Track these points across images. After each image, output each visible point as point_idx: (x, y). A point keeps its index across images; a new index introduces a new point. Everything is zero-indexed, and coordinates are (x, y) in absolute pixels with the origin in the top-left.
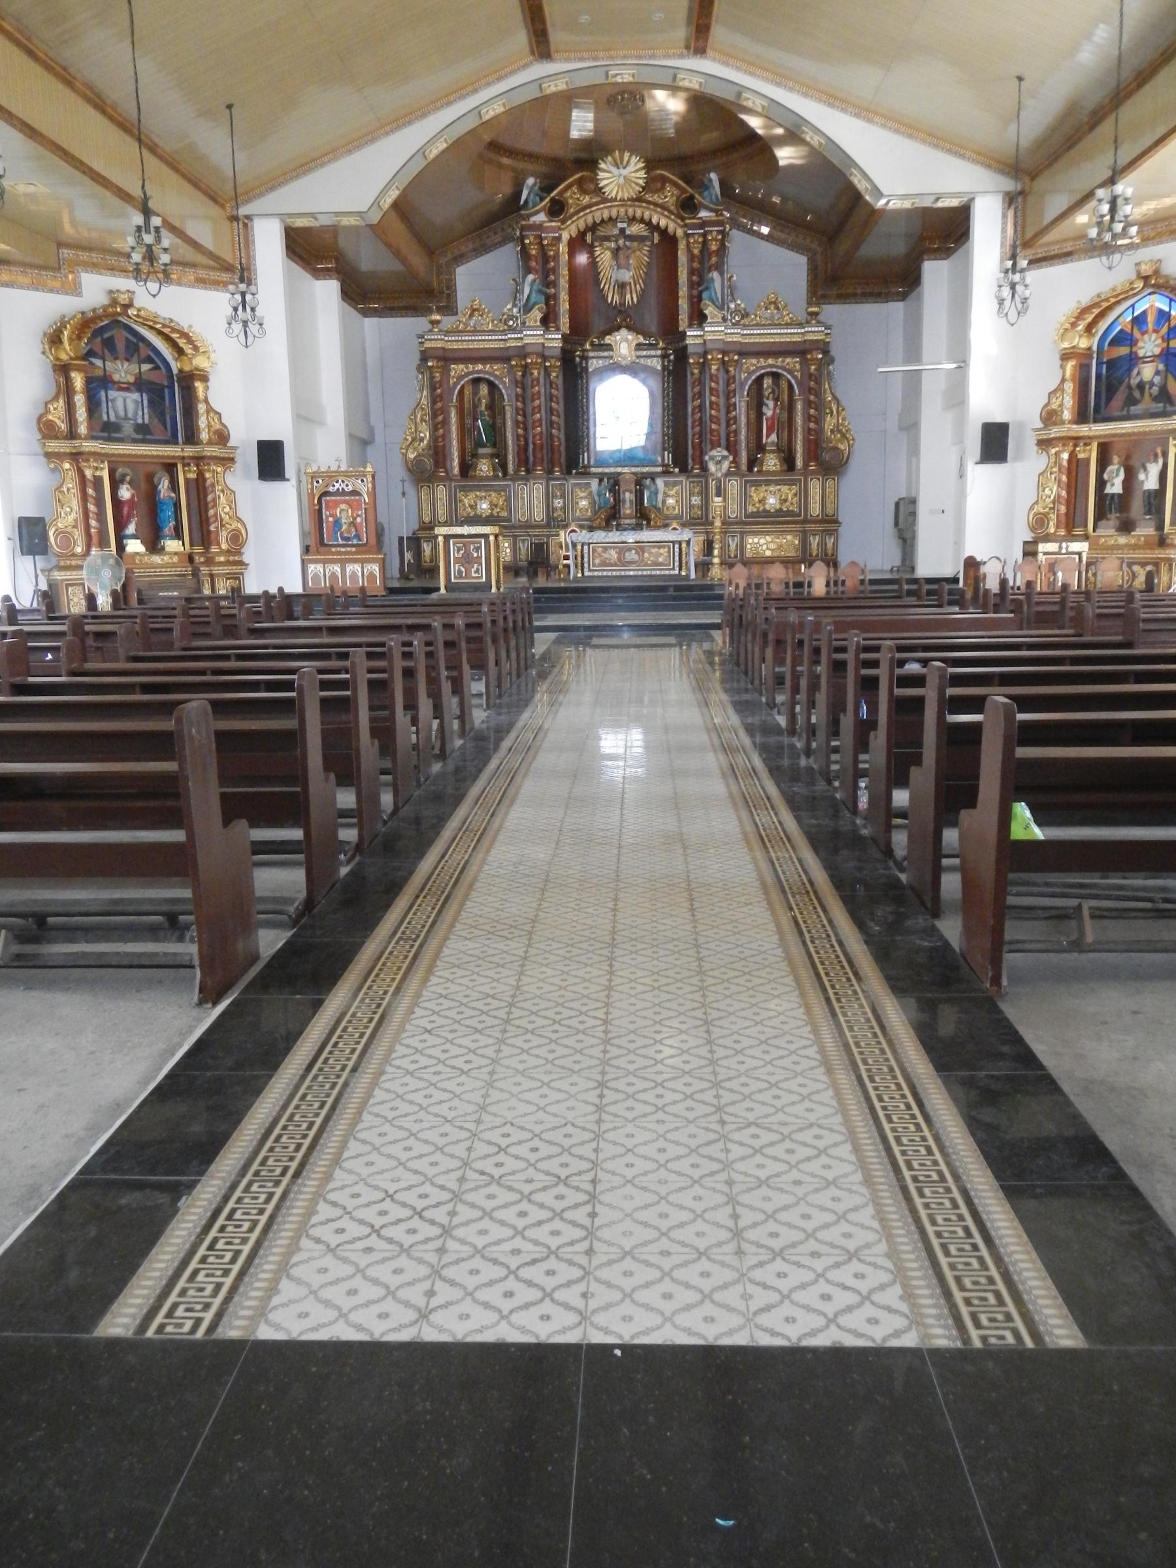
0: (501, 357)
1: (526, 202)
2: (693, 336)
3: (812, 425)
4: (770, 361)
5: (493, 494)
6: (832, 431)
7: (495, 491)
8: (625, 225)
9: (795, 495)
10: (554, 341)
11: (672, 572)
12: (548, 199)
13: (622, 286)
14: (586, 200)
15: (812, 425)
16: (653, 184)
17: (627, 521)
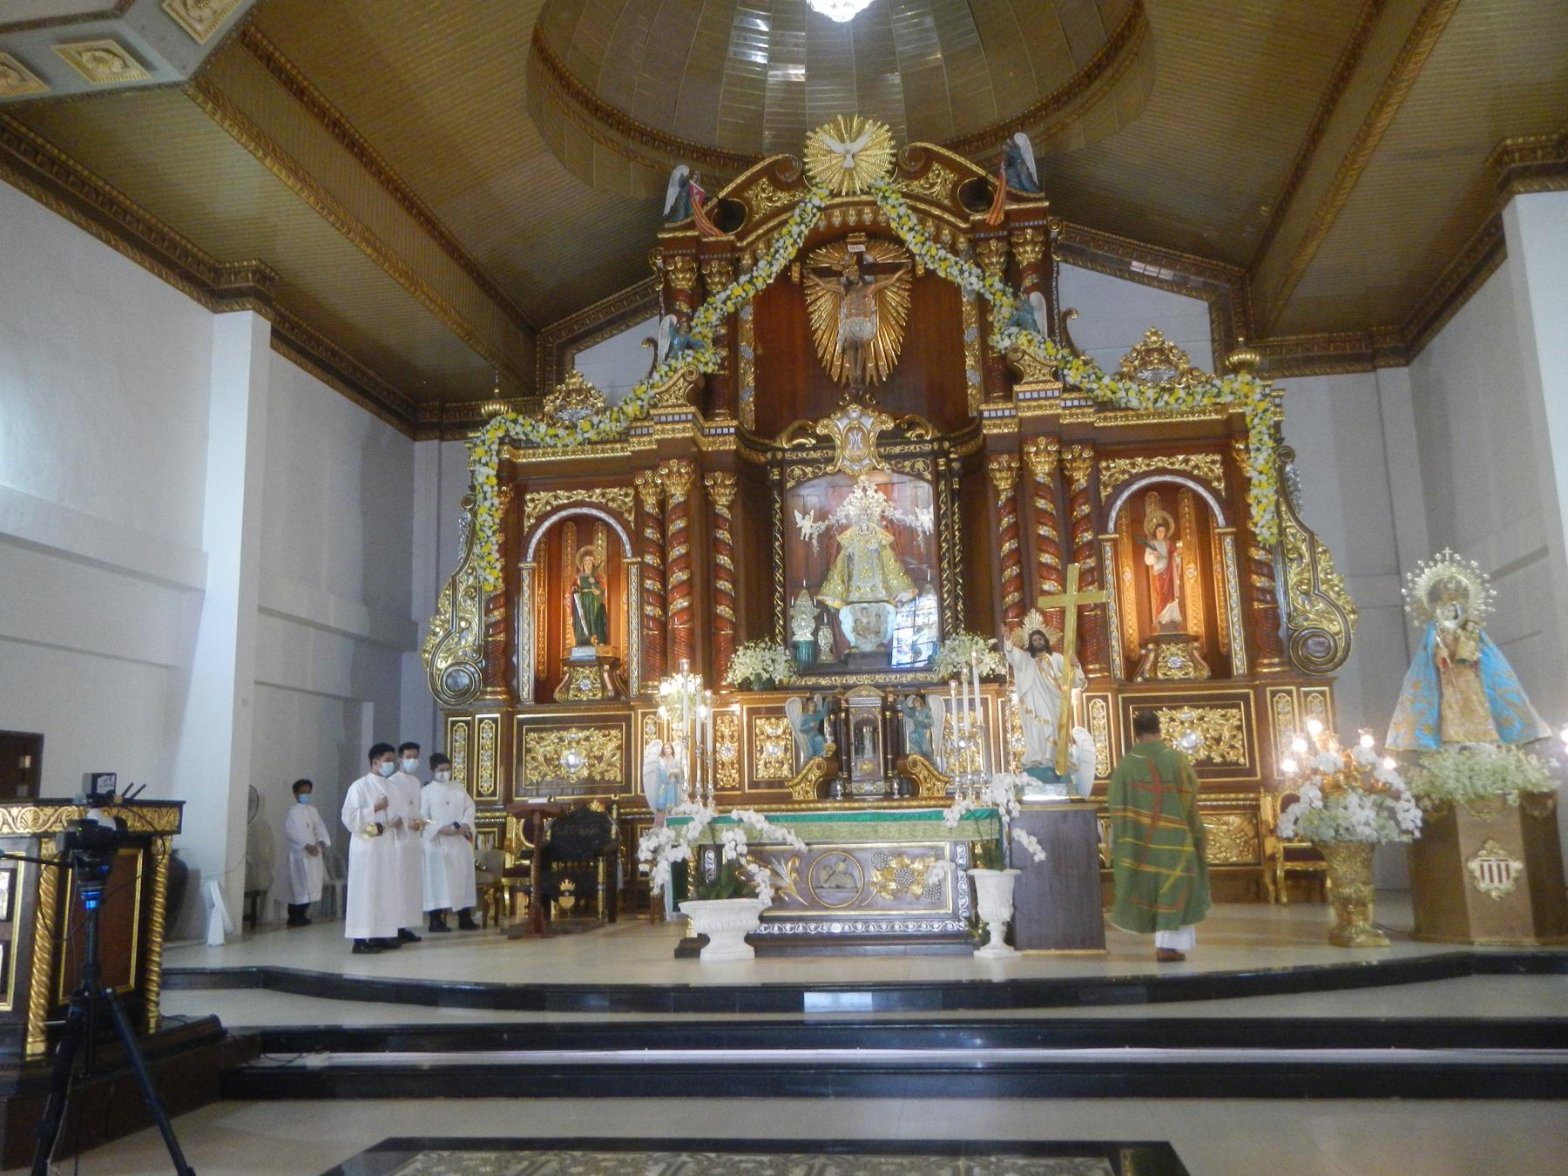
0: (621, 473)
1: (674, 209)
2: (997, 419)
3: (1259, 581)
4: (1160, 462)
5: (597, 736)
6: (1306, 593)
7: (599, 728)
8: (862, 248)
9: (1239, 728)
10: (722, 434)
11: (952, 926)
12: (715, 201)
13: (855, 347)
14: (783, 198)
15: (1259, 581)
16: (908, 165)
17: (867, 787)
